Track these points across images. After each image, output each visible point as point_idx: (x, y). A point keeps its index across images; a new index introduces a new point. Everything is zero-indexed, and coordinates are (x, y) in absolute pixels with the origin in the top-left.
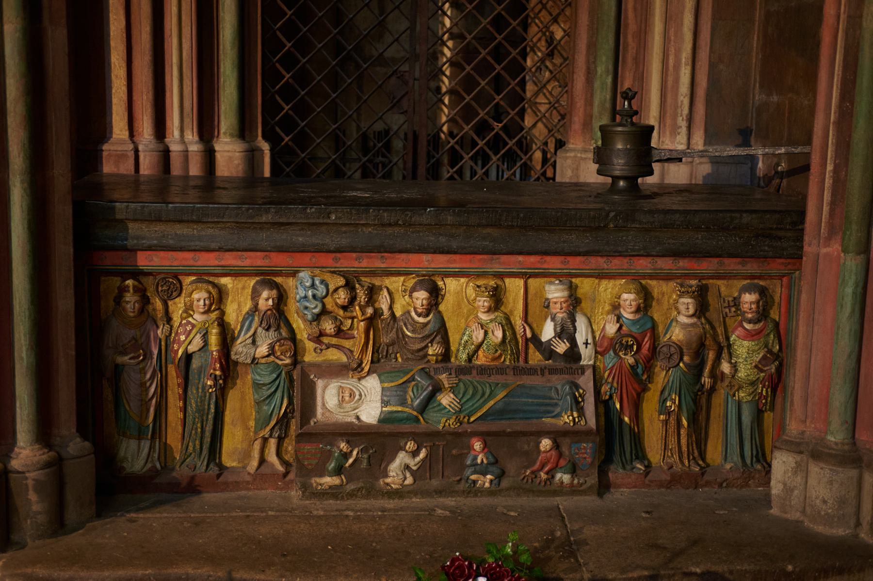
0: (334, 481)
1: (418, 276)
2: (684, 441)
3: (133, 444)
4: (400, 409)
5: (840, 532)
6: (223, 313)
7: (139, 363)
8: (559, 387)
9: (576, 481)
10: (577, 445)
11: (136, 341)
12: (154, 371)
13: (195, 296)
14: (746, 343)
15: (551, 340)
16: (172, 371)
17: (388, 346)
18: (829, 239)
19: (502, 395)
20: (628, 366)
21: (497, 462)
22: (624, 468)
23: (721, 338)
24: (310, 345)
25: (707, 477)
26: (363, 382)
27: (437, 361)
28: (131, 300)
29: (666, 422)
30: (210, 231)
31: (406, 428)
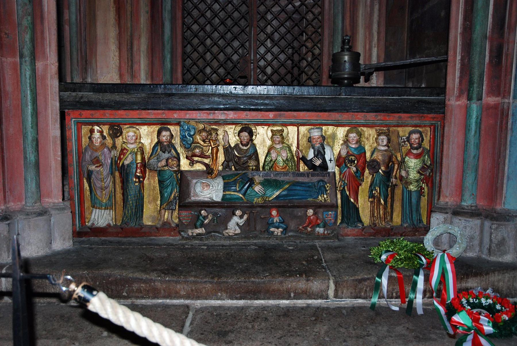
9: (326, 232)
10: (326, 213)
15: (312, 158)
20: (353, 172)
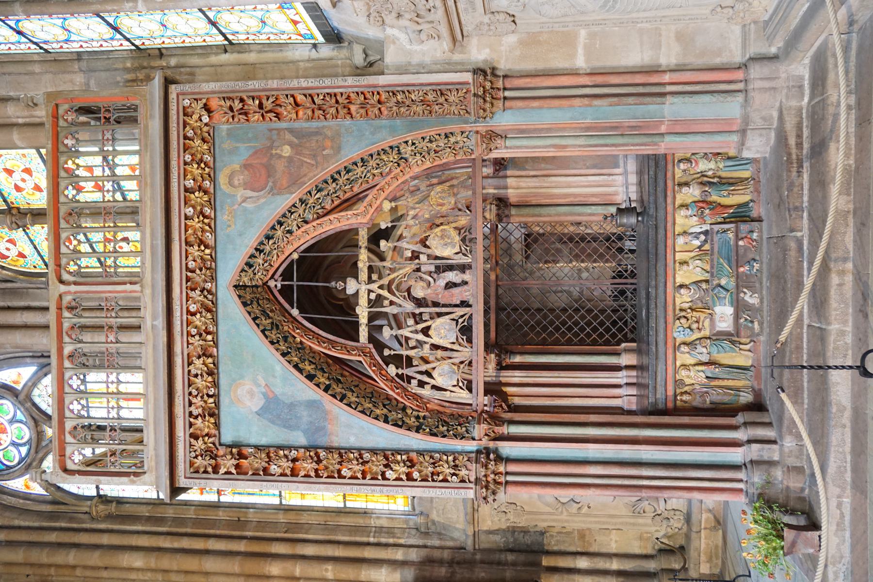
0: (756, 324)
2: (741, 188)
3: (741, 398)
5: (773, 134)
6: (690, 365)
13: (683, 374)
16: (713, 384)
18: (658, 145)
19: (721, 260)
23: (699, 175)
24: (703, 332)
28: (685, 398)
29: (733, 194)
31: (734, 297)
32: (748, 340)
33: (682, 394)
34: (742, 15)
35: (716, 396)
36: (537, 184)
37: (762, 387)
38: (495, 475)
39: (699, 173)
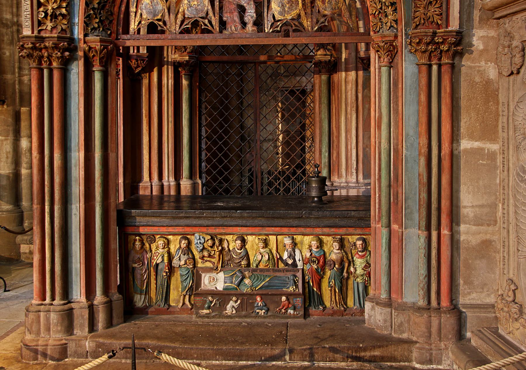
1: (237, 235)
2: (337, 298)
3: (139, 296)
4: (230, 285)
6: (169, 249)
7: (140, 267)
8: (289, 277)
10: (296, 299)
11: (140, 259)
12: (146, 270)
13: (159, 243)
14: (359, 260)
16: (152, 269)
17: (228, 261)
18: (379, 221)
19: (268, 279)
21: (266, 305)
22: (315, 308)
24: (200, 261)
25: (346, 312)
26: (218, 274)
27: (245, 267)
28: (138, 243)
29: (331, 290)
30: (164, 219)
32: (193, 303)
33: (142, 241)
34: (506, 309)
35: (141, 271)
36: (349, 101)
37: (149, 316)
38: (48, 58)
39: (353, 258)
